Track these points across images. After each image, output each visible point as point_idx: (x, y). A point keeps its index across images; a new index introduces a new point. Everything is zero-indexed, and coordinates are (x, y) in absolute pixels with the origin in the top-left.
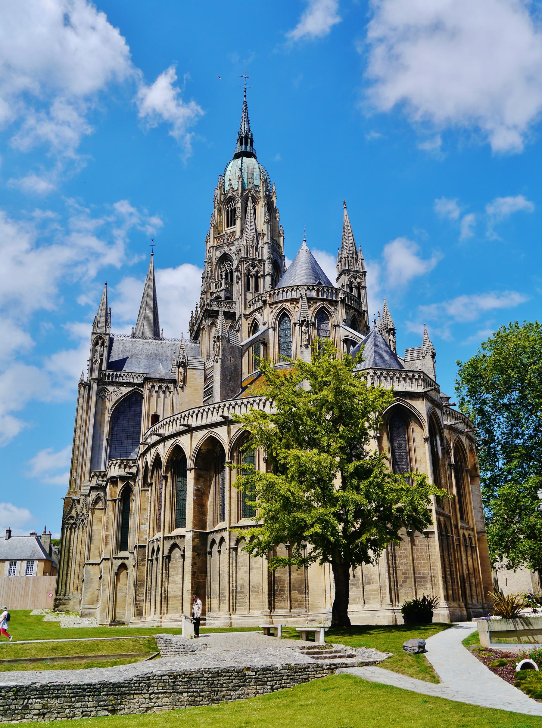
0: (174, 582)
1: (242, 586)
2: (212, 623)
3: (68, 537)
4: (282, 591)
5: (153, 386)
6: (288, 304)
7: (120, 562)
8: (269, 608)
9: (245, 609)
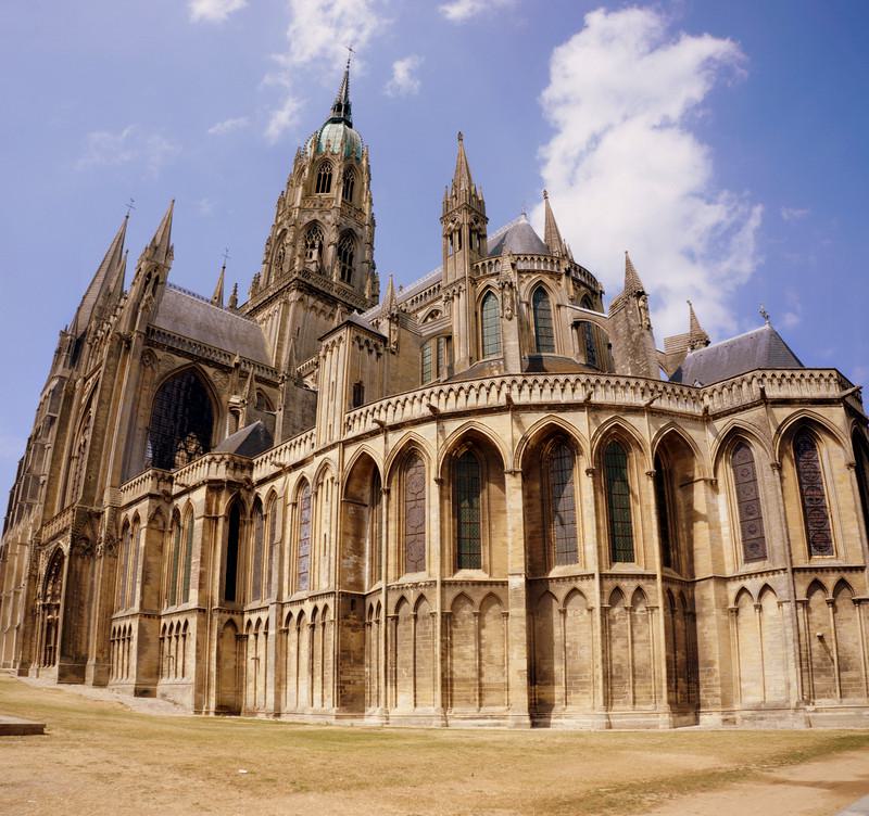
0: (462, 656)
1: (620, 666)
5: (358, 338)
7: (228, 616)
8: (443, 706)
9: (625, 703)
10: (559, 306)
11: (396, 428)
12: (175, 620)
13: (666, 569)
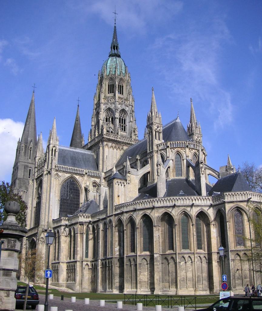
0: (144, 275)
1: (184, 278)
2: (167, 293)
3: (41, 248)
4: (200, 280)
6: (180, 149)
10: (183, 160)
11: (127, 212)
12: (71, 264)
13: (198, 250)
